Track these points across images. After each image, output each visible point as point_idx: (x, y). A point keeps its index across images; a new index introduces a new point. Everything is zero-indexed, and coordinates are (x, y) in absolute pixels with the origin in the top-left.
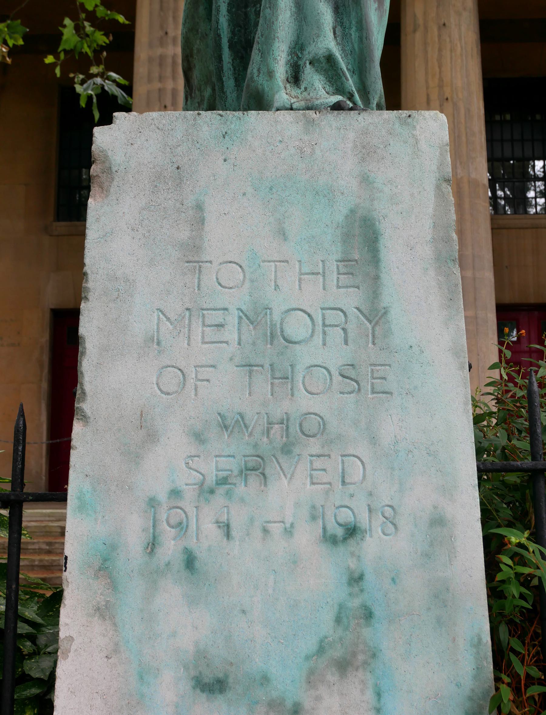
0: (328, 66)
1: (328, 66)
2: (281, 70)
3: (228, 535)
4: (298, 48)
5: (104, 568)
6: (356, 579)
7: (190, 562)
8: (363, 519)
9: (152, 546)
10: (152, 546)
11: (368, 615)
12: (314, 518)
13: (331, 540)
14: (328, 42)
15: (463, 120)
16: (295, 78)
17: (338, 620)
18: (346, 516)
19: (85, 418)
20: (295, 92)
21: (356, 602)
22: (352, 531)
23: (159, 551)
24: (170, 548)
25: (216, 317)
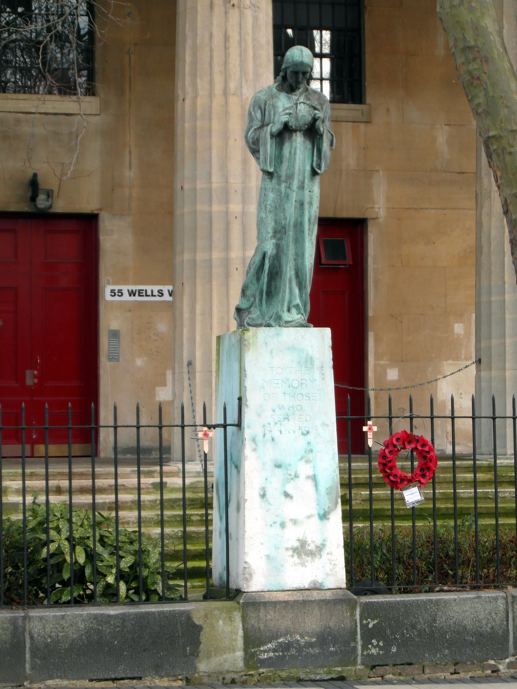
0: (297, 306)
1: (297, 306)
2: (285, 309)
3: (281, 433)
4: (290, 302)
5: (254, 440)
6: (309, 443)
7: (273, 439)
8: (310, 431)
9: (264, 436)
10: (264, 436)
11: (311, 451)
12: (300, 429)
13: (303, 434)
14: (298, 301)
15: (250, 31)
16: (289, 310)
17: (305, 452)
18: (307, 430)
19: (247, 406)
20: (289, 314)
21: (309, 448)
22: (308, 432)
23: (266, 437)
24: (268, 436)
25: (276, 382)
